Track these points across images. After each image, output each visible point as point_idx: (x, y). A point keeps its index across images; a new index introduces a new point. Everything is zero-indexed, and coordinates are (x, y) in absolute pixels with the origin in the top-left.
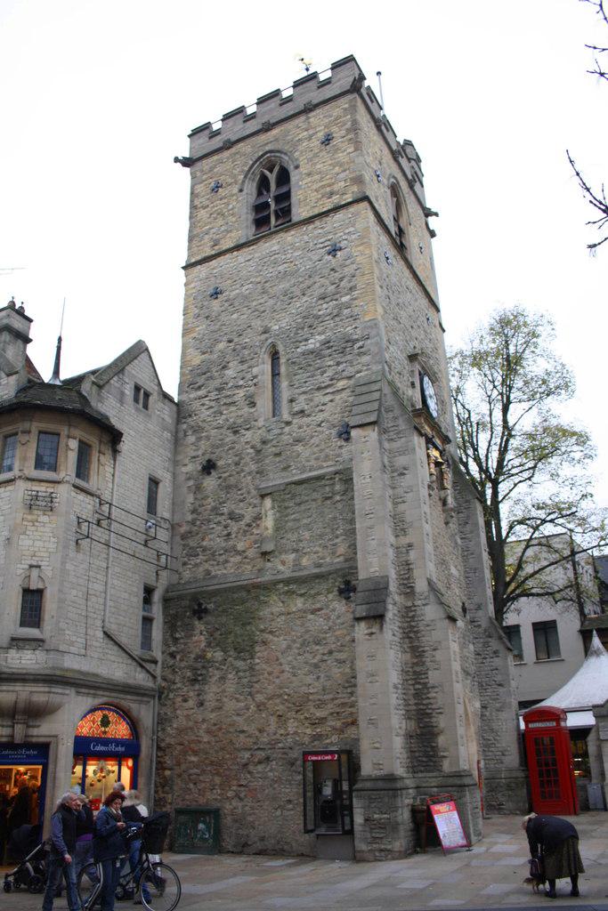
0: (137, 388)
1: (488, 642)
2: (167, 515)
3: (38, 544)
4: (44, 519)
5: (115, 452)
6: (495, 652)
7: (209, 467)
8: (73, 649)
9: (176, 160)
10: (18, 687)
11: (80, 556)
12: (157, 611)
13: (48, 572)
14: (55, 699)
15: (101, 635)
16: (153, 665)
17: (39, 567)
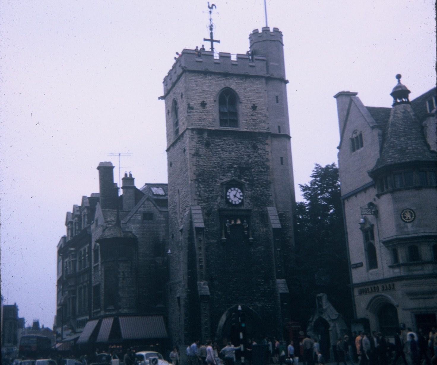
9: (159, 98)
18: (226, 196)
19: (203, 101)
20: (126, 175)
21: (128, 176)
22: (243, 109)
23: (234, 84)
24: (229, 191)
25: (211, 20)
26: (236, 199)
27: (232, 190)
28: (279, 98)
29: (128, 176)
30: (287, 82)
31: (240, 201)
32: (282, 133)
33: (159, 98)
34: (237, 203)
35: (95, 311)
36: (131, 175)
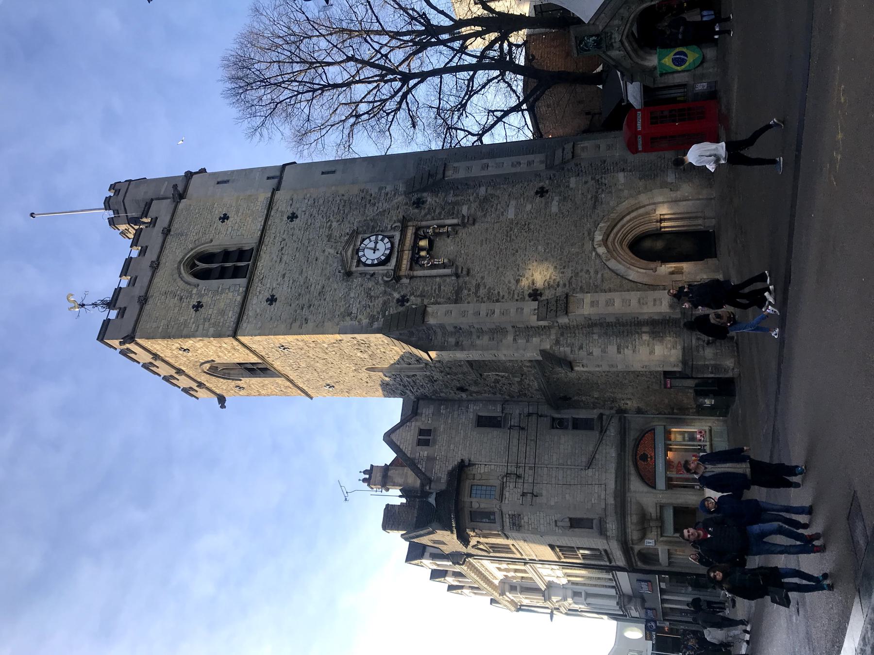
0: (420, 443)
1: (568, 170)
2: (499, 408)
3: (542, 522)
4: (526, 519)
5: (471, 464)
6: (577, 165)
7: (462, 389)
8: (603, 497)
9: (223, 406)
10: (629, 530)
11: (544, 493)
12: (568, 414)
13: (558, 516)
14: (634, 507)
15: (590, 472)
16: (604, 417)
17: (556, 521)
18: (373, 265)
19: (194, 307)
20: (364, 480)
21: (367, 476)
22: (224, 238)
23: (177, 252)
24: (363, 259)
25: (95, 305)
26: (380, 245)
27: (364, 255)
28: (219, 180)
29: (367, 476)
30: (203, 171)
31: (386, 240)
32: (278, 174)
33: (223, 406)
34: (389, 245)
35: (606, 559)
36: (365, 472)
